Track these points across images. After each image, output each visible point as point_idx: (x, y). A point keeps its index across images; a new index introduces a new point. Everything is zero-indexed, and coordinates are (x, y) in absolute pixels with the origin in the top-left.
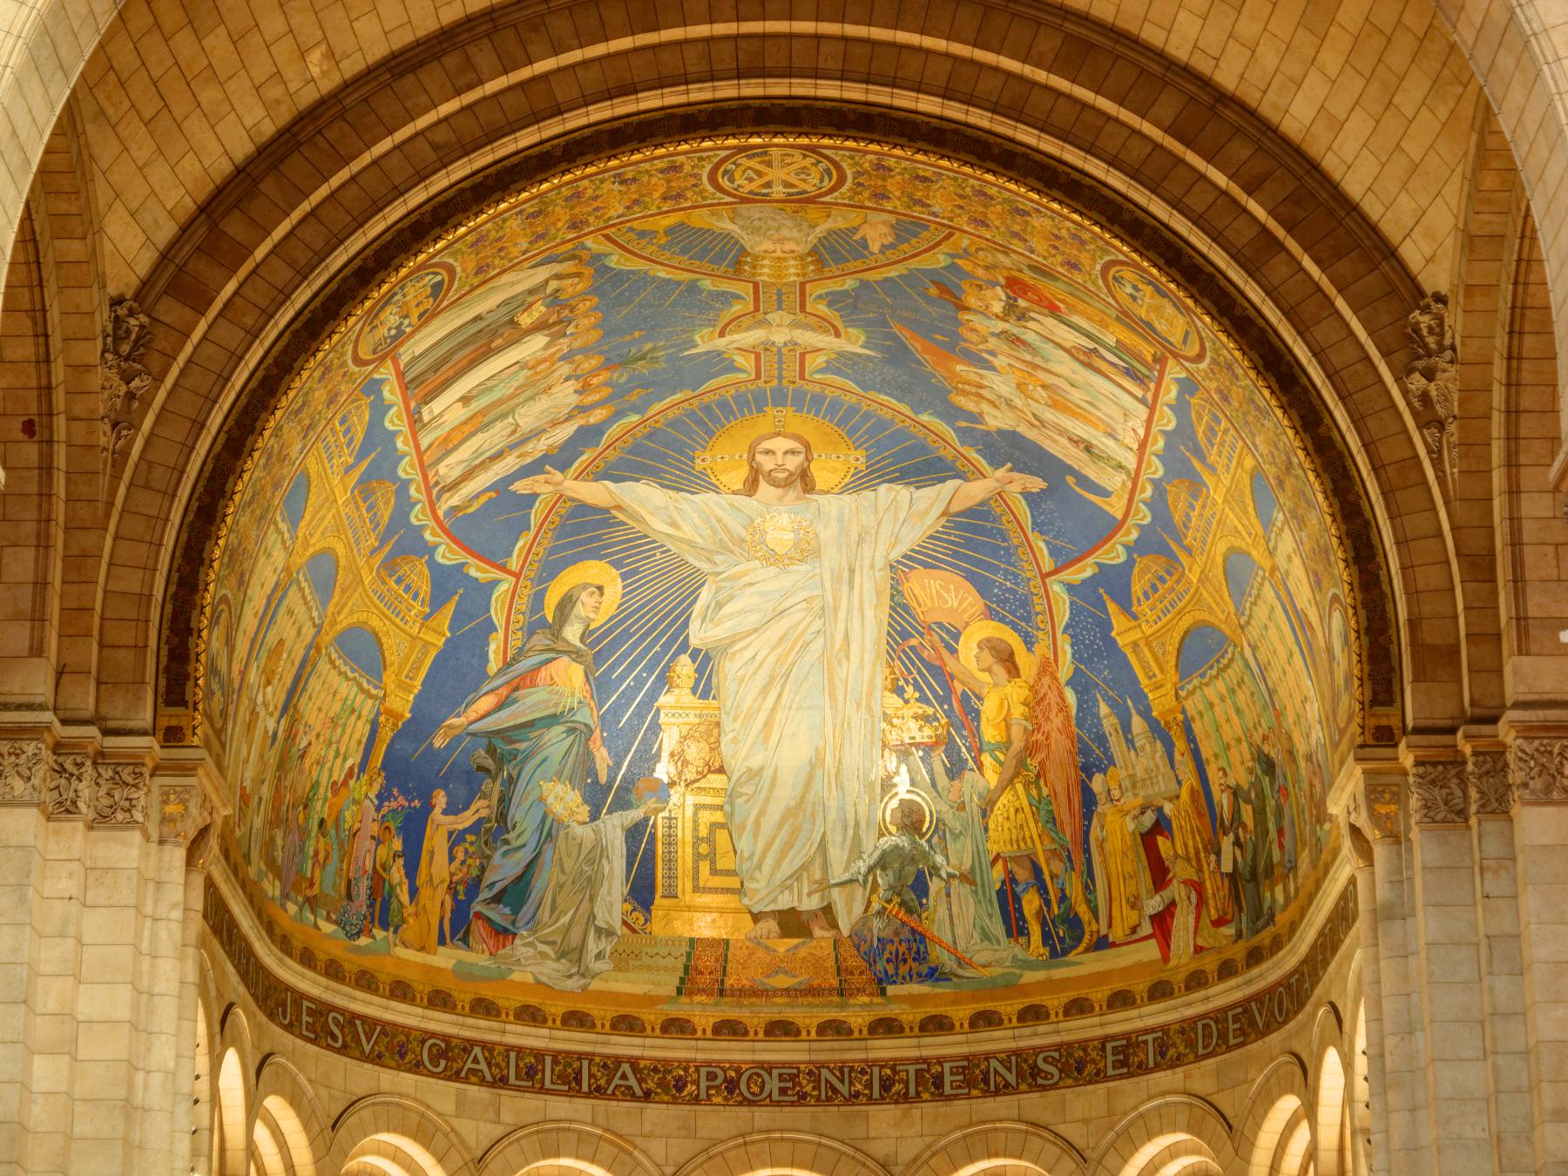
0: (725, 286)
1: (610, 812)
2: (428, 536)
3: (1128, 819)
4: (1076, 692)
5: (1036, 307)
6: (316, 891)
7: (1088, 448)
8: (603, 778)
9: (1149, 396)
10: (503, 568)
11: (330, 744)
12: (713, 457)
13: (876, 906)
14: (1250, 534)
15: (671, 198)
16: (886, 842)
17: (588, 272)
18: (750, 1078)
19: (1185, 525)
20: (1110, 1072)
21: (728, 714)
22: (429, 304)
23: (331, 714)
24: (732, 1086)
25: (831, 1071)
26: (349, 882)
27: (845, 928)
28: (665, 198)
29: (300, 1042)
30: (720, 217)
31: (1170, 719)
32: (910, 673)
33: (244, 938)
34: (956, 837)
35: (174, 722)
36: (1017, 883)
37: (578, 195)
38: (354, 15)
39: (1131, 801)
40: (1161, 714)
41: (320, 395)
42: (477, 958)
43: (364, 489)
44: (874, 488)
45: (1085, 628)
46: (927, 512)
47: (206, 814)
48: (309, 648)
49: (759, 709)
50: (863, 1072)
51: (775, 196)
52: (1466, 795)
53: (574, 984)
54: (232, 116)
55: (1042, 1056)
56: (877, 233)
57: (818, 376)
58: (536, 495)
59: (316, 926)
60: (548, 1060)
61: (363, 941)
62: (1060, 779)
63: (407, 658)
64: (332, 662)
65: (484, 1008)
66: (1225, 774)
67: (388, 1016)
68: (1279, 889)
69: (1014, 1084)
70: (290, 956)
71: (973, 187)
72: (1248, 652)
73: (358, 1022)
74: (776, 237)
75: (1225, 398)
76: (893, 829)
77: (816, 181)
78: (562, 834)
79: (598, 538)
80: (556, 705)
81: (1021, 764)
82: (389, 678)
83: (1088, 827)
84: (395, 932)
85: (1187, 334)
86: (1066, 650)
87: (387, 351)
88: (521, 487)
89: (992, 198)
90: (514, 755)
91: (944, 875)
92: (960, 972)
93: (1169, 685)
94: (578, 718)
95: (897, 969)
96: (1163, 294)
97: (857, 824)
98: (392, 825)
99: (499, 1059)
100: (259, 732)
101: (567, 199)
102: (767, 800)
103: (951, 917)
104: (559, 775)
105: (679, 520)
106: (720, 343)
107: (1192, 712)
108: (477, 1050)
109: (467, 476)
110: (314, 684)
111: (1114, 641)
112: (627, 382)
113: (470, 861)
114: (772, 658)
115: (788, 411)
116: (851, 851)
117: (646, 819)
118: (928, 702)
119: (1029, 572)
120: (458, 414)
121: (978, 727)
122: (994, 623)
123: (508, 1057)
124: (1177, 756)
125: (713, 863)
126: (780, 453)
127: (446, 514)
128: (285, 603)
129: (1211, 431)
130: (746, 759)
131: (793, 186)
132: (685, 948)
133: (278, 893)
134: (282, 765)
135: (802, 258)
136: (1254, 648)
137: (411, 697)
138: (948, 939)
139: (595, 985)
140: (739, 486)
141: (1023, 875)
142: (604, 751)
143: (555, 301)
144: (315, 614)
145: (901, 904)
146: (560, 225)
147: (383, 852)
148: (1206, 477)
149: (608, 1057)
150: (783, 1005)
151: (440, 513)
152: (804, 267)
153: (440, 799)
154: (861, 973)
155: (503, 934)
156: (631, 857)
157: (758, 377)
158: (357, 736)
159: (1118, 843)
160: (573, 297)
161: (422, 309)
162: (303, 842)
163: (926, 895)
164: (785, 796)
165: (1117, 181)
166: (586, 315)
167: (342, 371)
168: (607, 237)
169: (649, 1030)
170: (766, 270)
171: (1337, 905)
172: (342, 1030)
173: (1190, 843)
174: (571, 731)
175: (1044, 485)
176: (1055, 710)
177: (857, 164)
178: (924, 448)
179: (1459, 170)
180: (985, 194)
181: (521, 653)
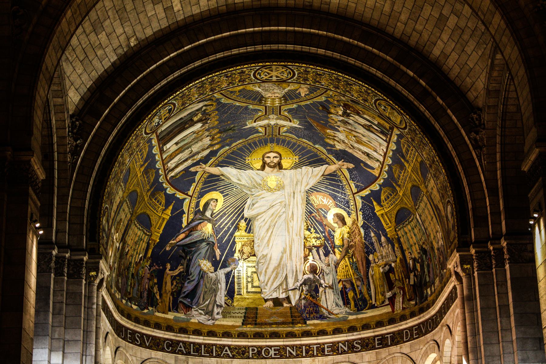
0: (257, 107)
1: (220, 269)
2: (164, 185)
3: (381, 268)
4: (364, 229)
5: (353, 113)
7: (368, 155)
8: (218, 258)
9: (388, 139)
10: (187, 194)
11: (134, 250)
12: (251, 159)
13: (303, 296)
14: (419, 181)
15: (242, 81)
16: (306, 277)
17: (214, 104)
18: (265, 350)
19: (398, 178)
20: (377, 347)
21: (256, 238)
22: (167, 115)
23: (135, 241)
24: (259, 353)
25: (290, 348)
26: (141, 292)
27: (294, 305)
28: (239, 81)
29: (127, 343)
30: (255, 86)
31: (393, 237)
32: (312, 224)
33: (111, 312)
34: (327, 274)
35: (92, 247)
36: (347, 288)
37: (213, 81)
38: (144, 27)
39: (381, 262)
40: (390, 236)
41: (135, 144)
42: (181, 316)
43: (146, 172)
44: (301, 168)
45: (366, 210)
46: (317, 175)
47: (102, 275)
48: (128, 221)
49: (266, 236)
50: (300, 348)
51: (273, 80)
52: (491, 262)
53: (210, 322)
54: (107, 59)
55: (355, 342)
56: (303, 91)
57: (284, 134)
58: (197, 172)
60: (203, 346)
61: (146, 311)
62: (358, 257)
63: (158, 223)
64: (136, 225)
65: (183, 331)
66: (411, 254)
67: (154, 334)
68: (429, 290)
69: (347, 351)
70: (124, 317)
71: (335, 77)
72: (418, 217)
73: (144, 336)
74: (272, 92)
75: (413, 140)
76: (308, 272)
77: (286, 76)
78: (206, 276)
79: (216, 185)
80: (204, 236)
81: (347, 252)
82: (153, 229)
83: (368, 271)
84: (155, 308)
85: (401, 121)
86: (360, 217)
87: (154, 131)
88: (193, 169)
89: (340, 80)
90: (191, 251)
91: (324, 286)
92: (329, 316)
93: (393, 227)
94: (210, 240)
95: (310, 315)
96: (394, 109)
97: (297, 271)
98: (154, 274)
99: (188, 346)
100: (114, 247)
101: (210, 82)
102: (269, 264)
103: (326, 299)
104: (204, 258)
105: (241, 178)
106: (254, 125)
107: (400, 235)
108: (181, 344)
109: (176, 167)
110: (130, 232)
111: (375, 214)
112: (226, 136)
113: (178, 285)
114: (270, 220)
115: (274, 145)
116: (295, 279)
117: (232, 271)
118: (318, 233)
119: (349, 192)
120: (175, 148)
121: (334, 241)
122: (338, 209)
123: (190, 346)
124: (396, 249)
125: (252, 284)
126: (272, 158)
127: (170, 178)
128: (122, 207)
129: (407, 150)
130: (262, 252)
131: (279, 77)
132: (244, 311)
133: (120, 297)
134: (121, 257)
135: (280, 98)
136: (420, 216)
137: (159, 235)
138: (325, 306)
139: (217, 323)
140: (259, 168)
141: (348, 286)
142: (218, 250)
143: (204, 113)
144: (131, 210)
145: (311, 296)
146: (207, 90)
147: (151, 283)
148: (406, 164)
149: (221, 345)
150: (275, 327)
151: (168, 178)
152: (281, 101)
153: (169, 266)
154: (299, 317)
155: (188, 308)
156: (227, 282)
157: (266, 134)
158: (143, 247)
159: (378, 275)
160: (210, 112)
161: (165, 117)
162: (127, 281)
163: (319, 293)
164: (274, 263)
165: (379, 74)
166: (214, 117)
167: (141, 136)
168: (221, 94)
169: (234, 336)
170: (269, 102)
171: (449, 295)
172: (139, 339)
173: (400, 275)
174: (208, 244)
175: (354, 166)
176: (357, 235)
177: (299, 70)
178: (316, 155)
179: (485, 70)
180: (338, 79)
181: (193, 220)
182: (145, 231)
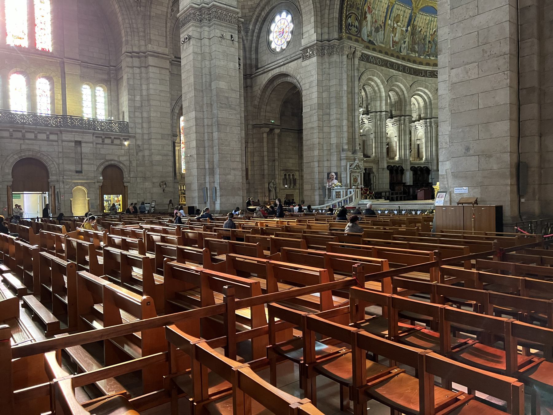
6: (429, 53)
23: (426, 23)
59: (430, 58)
134: (413, 34)
144: (408, 8)
162: (424, 47)
182: (433, 16)
